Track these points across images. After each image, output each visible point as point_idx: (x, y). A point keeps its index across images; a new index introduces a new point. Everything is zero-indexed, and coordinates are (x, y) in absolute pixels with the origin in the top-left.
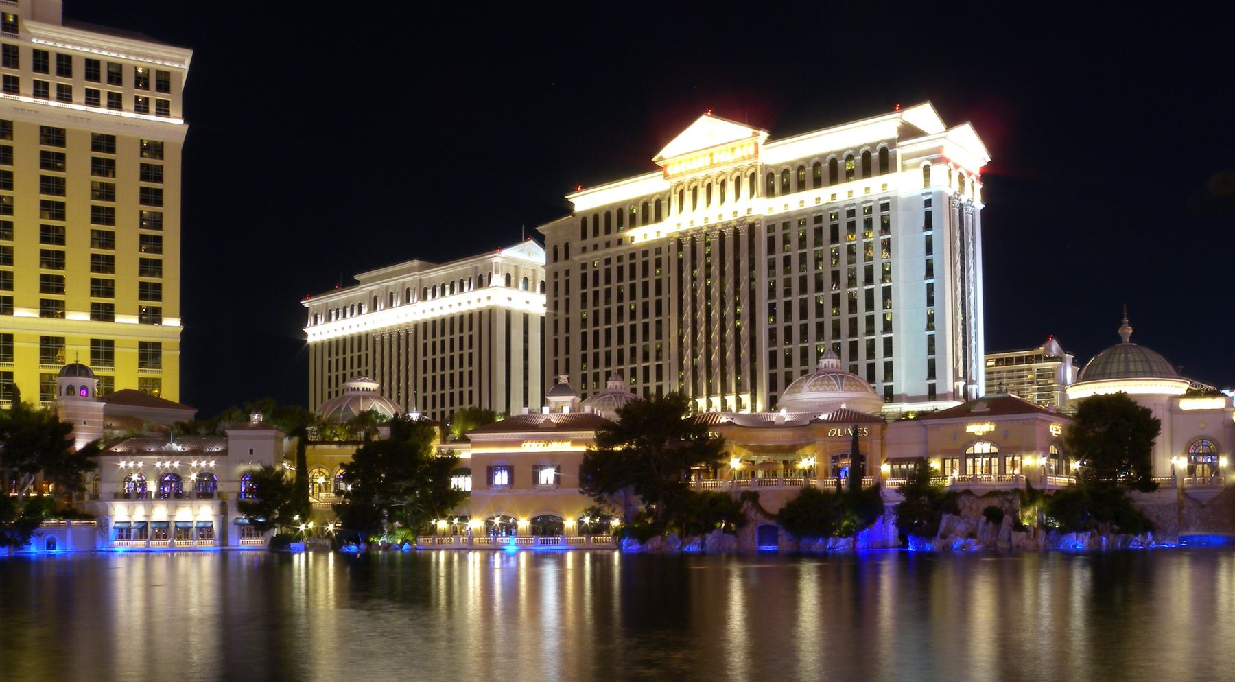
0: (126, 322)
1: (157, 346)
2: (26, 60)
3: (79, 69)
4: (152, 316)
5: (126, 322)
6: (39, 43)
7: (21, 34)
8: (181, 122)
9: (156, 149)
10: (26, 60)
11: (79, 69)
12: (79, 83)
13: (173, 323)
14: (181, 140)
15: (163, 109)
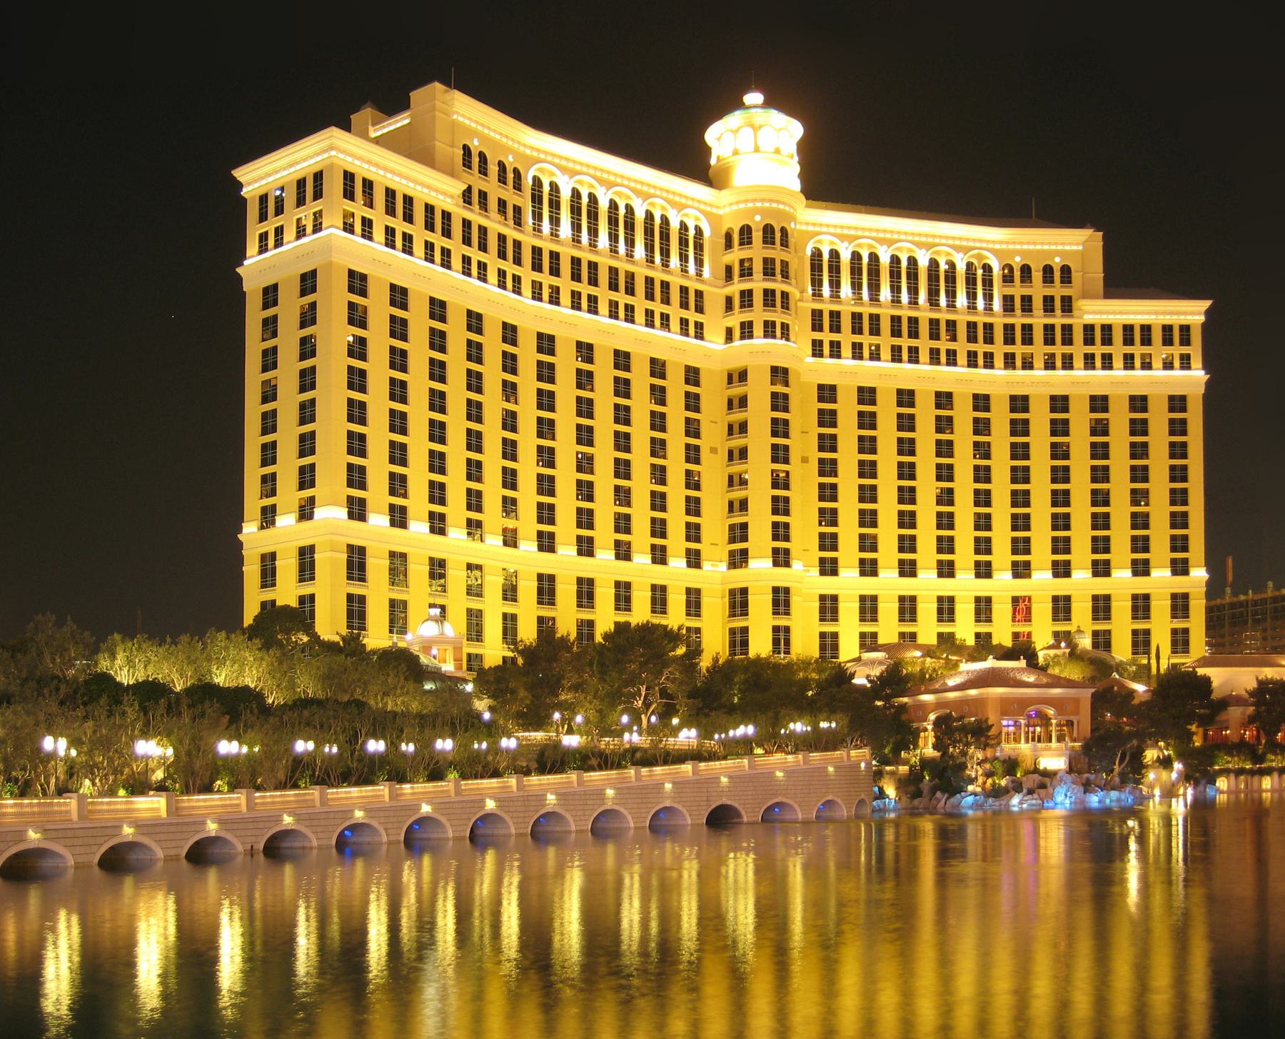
0: (1161, 574)
1: (1186, 596)
2: (1078, 336)
3: (1118, 336)
4: (1180, 568)
5: (1161, 574)
6: (1089, 319)
7: (1075, 312)
8: (1202, 373)
9: (1178, 403)
10: (1078, 336)
11: (1118, 336)
12: (1118, 350)
13: (1199, 574)
14: (1202, 390)
15: (1186, 362)
